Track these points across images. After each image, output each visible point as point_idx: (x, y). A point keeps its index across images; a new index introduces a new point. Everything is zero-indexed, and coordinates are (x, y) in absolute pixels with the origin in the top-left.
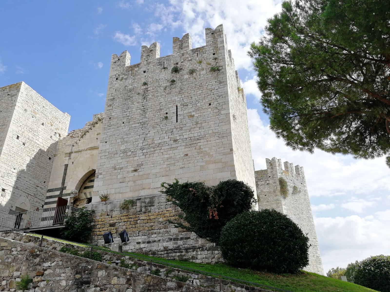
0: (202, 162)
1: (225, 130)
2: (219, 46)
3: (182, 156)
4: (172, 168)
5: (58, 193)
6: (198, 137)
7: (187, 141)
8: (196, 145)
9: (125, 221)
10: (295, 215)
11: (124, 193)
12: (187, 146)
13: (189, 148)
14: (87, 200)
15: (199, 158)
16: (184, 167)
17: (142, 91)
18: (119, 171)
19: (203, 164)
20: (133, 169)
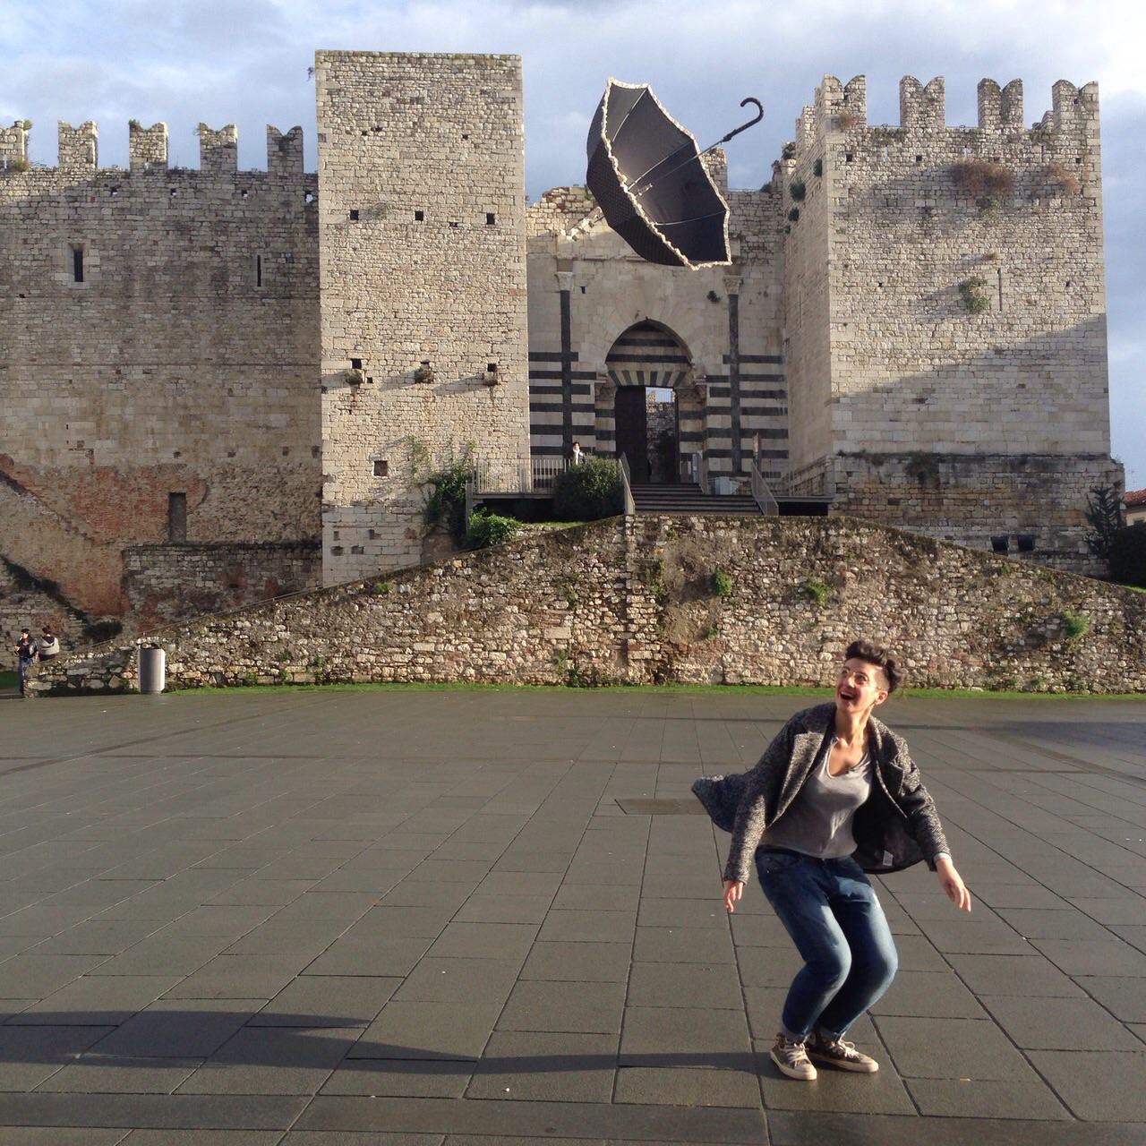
0: (1053, 405)
2: (1090, 142)
4: (995, 407)
5: (556, 366)
6: (1044, 353)
7: (1022, 357)
8: (1040, 368)
12: (1022, 369)
14: (616, 389)
15: (1046, 396)
16: (1018, 410)
17: (917, 211)
18: (885, 395)
20: (914, 396)
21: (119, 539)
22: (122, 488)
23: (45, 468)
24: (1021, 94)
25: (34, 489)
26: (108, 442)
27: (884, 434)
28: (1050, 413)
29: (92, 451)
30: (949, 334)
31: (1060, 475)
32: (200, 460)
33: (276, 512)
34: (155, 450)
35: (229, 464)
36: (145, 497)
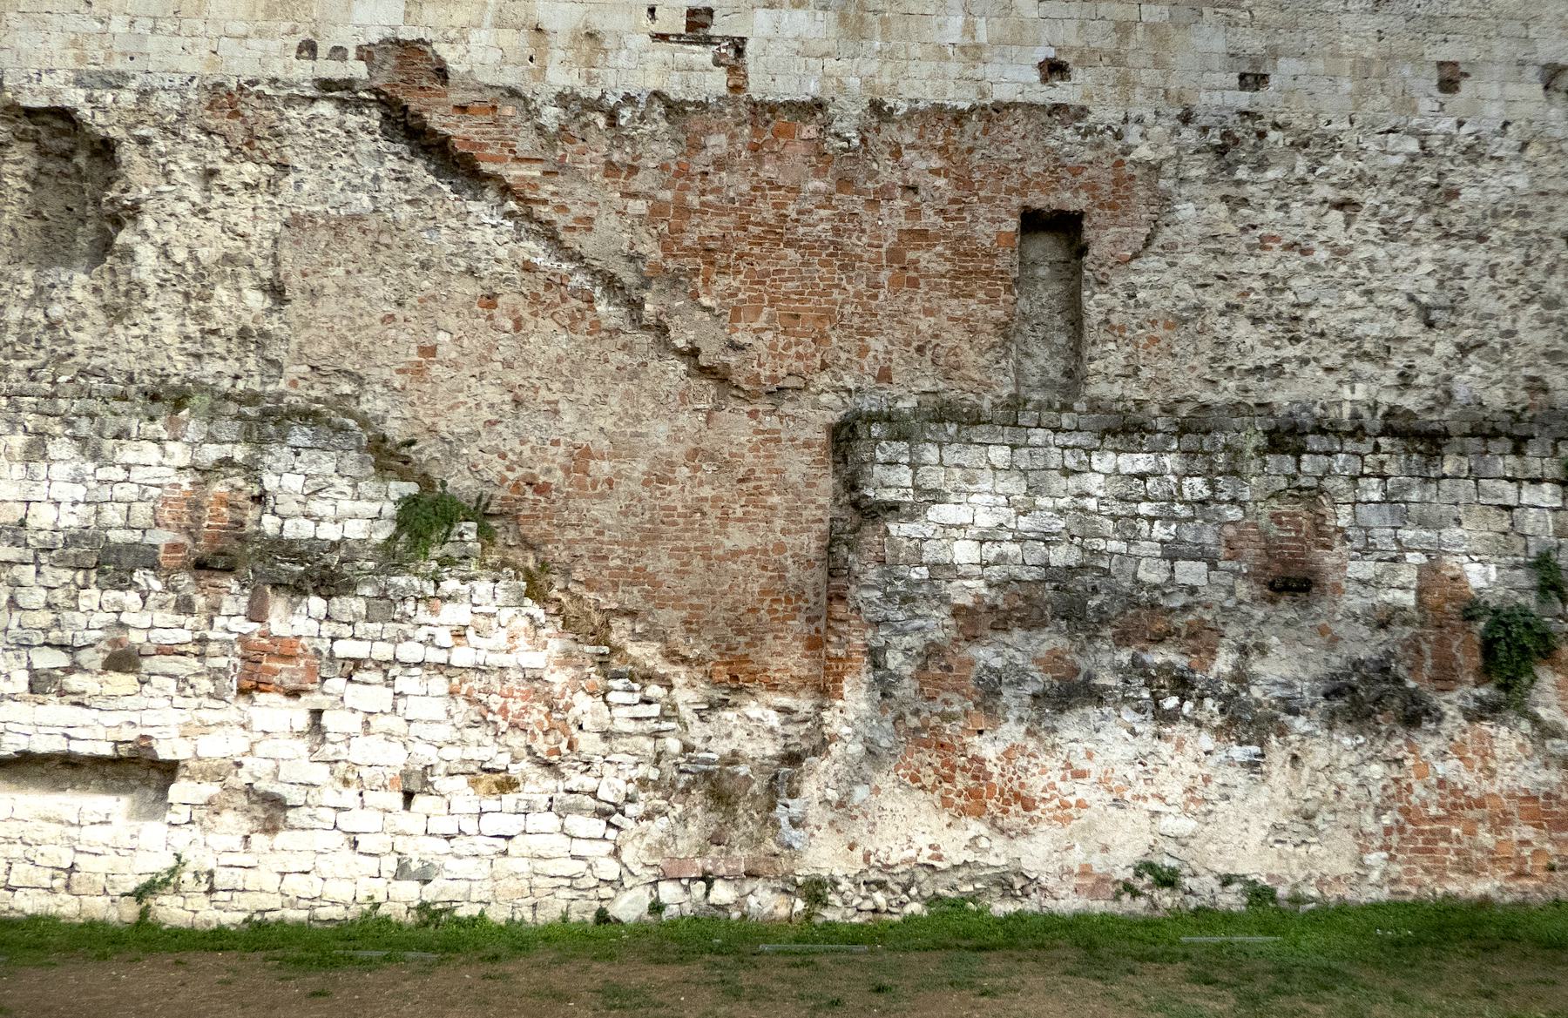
21: (825, 379)
22: (844, 183)
23: (562, 99)
25: (514, 173)
26: (800, 14)
29: (739, 46)
32: (1138, 95)
33: (1424, 299)
34: (973, 52)
35: (1245, 114)
36: (930, 220)
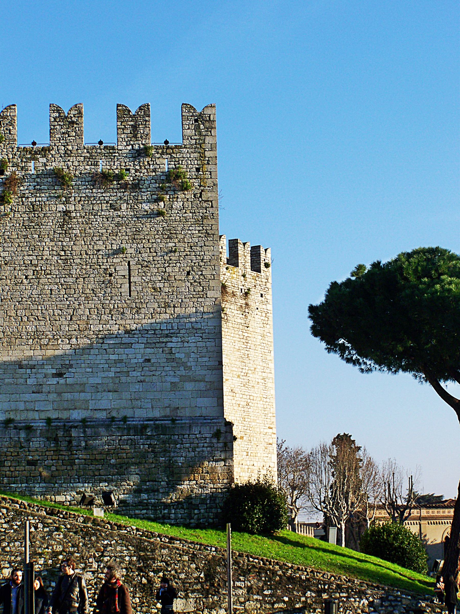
1: (212, 328)
3: (140, 361)
4: (123, 379)
6: (167, 332)
9: (53, 458)
10: (239, 376)
11: (43, 411)
12: (148, 345)
13: (153, 348)
17: (59, 215)
18: (29, 371)
19: (177, 380)
24: (149, 116)
27: (27, 404)
28: (172, 383)
30: (85, 318)
31: (177, 437)
